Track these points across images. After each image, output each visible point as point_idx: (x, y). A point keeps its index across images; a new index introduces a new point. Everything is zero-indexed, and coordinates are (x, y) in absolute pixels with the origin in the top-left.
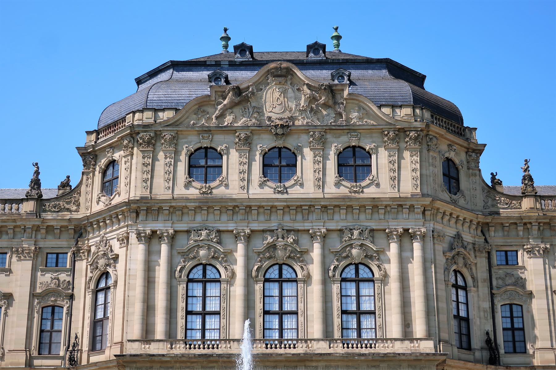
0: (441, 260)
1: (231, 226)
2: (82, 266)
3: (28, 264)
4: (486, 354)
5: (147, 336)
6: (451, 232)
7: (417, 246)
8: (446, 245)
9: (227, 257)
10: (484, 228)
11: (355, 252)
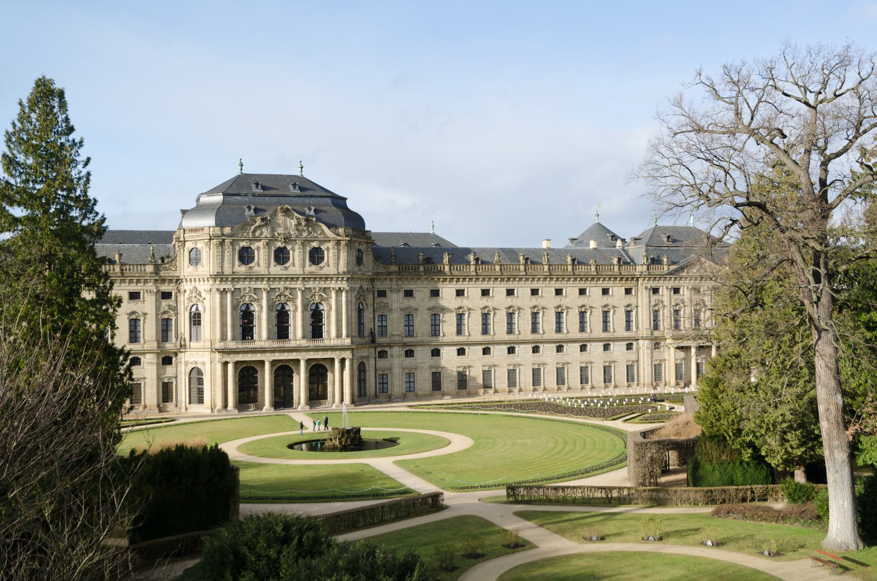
0: (354, 299)
1: (260, 286)
2: (181, 298)
3: (154, 298)
4: (370, 338)
5: (223, 338)
6: (358, 286)
7: (344, 294)
8: (356, 292)
9: (258, 300)
10: (372, 280)
11: (317, 298)
